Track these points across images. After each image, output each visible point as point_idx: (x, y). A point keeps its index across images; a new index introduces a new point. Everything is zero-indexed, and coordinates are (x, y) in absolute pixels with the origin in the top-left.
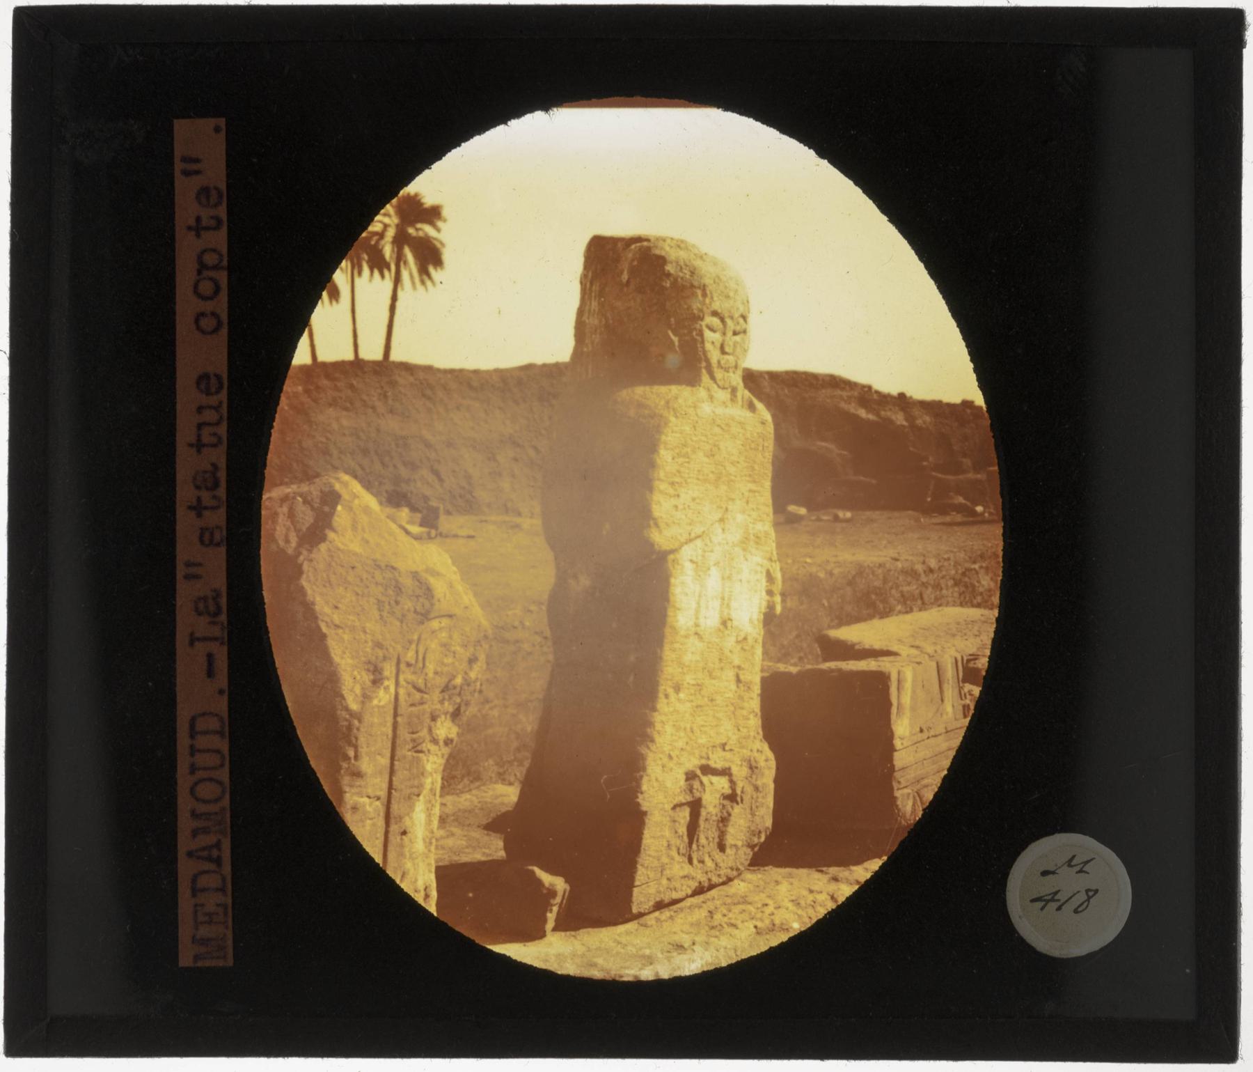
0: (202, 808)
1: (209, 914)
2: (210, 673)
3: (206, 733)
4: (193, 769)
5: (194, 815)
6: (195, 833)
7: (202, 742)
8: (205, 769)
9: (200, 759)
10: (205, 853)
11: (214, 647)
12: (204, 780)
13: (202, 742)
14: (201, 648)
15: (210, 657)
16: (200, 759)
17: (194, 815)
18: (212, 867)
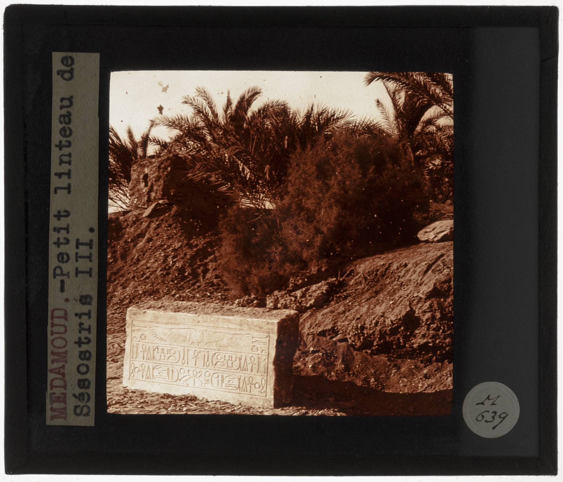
0: (56, 350)
1: (58, 398)
2: (62, 290)
4: (52, 333)
5: (53, 353)
6: (53, 361)
7: (56, 321)
8: (58, 333)
9: (55, 329)
11: (65, 278)
12: (57, 338)
13: (56, 321)
14: (59, 278)
15: (62, 282)
16: (55, 329)
17: (53, 353)
18: (60, 376)
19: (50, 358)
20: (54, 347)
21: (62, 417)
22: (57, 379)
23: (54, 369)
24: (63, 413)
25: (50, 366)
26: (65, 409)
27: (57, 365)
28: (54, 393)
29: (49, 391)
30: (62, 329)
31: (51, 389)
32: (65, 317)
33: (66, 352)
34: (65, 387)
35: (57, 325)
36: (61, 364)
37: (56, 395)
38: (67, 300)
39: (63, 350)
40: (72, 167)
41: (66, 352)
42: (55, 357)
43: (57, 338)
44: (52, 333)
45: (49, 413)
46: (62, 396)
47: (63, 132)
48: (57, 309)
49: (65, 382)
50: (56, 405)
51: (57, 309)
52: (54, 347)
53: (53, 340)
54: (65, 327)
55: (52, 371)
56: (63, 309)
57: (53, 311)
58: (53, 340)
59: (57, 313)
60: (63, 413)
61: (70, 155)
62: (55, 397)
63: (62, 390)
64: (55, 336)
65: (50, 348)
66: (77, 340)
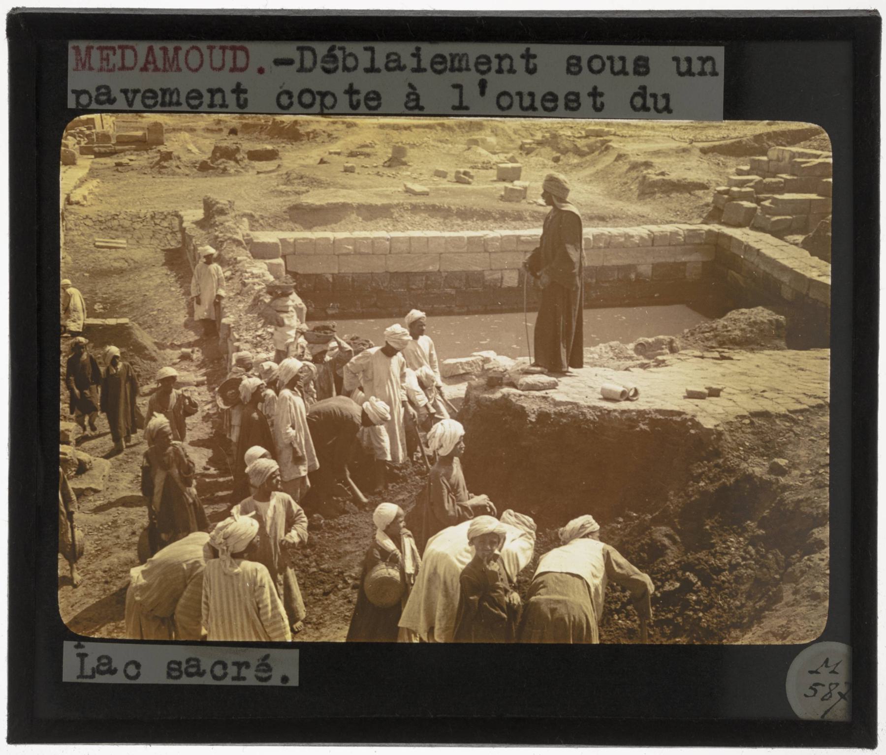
0: (182, 55)
1: (108, 59)
3: (235, 58)
5: (177, 49)
6: (165, 50)
7: (229, 54)
9: (217, 53)
10: (150, 59)
11: (297, 65)
12: (202, 55)
14: (296, 56)
15: (290, 62)
17: (177, 49)
18: (141, 62)
19: (171, 45)
20: (188, 52)
21: (77, 65)
22: (136, 55)
23: (153, 53)
24: (84, 65)
25: (157, 46)
26: (91, 69)
27: (159, 53)
28: (114, 54)
29: (115, 44)
30: (217, 63)
31: (120, 47)
32: (232, 70)
33: (179, 69)
34: (123, 68)
35: (224, 53)
36: (160, 64)
37: (111, 56)
38: (261, 71)
39: (182, 65)
40: (407, 73)
41: (179, 69)
42: (171, 53)
43: (202, 55)
44: (211, 48)
45: (83, 45)
46: (111, 66)
47: (439, 60)
48: (248, 57)
49: (132, 68)
50: (95, 55)
51: (248, 57)
52: (188, 52)
53: (198, 49)
54: (220, 69)
55: (151, 49)
56: (247, 64)
57: (243, 49)
58: (198, 49)
59: (240, 55)
60: (85, 65)
61: (512, 71)
62: (108, 55)
63: (120, 65)
64: (206, 52)
65: (185, 45)
66: (599, 90)
